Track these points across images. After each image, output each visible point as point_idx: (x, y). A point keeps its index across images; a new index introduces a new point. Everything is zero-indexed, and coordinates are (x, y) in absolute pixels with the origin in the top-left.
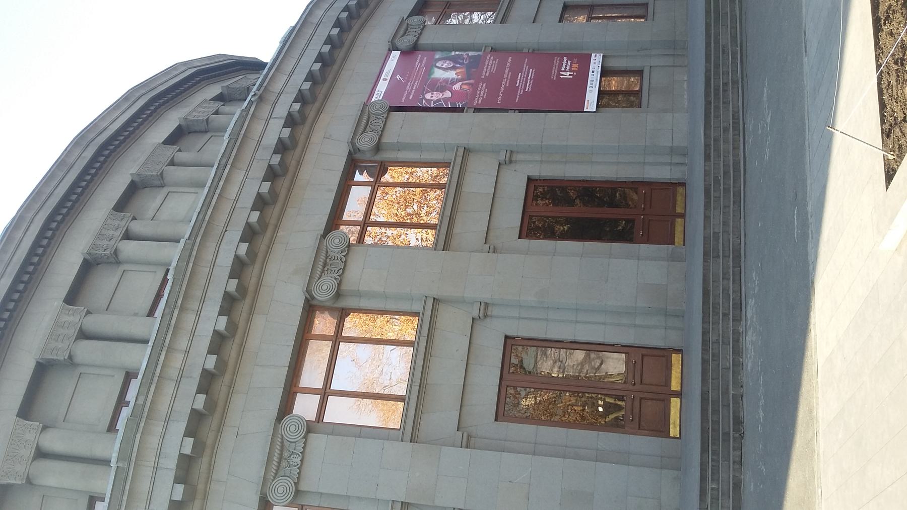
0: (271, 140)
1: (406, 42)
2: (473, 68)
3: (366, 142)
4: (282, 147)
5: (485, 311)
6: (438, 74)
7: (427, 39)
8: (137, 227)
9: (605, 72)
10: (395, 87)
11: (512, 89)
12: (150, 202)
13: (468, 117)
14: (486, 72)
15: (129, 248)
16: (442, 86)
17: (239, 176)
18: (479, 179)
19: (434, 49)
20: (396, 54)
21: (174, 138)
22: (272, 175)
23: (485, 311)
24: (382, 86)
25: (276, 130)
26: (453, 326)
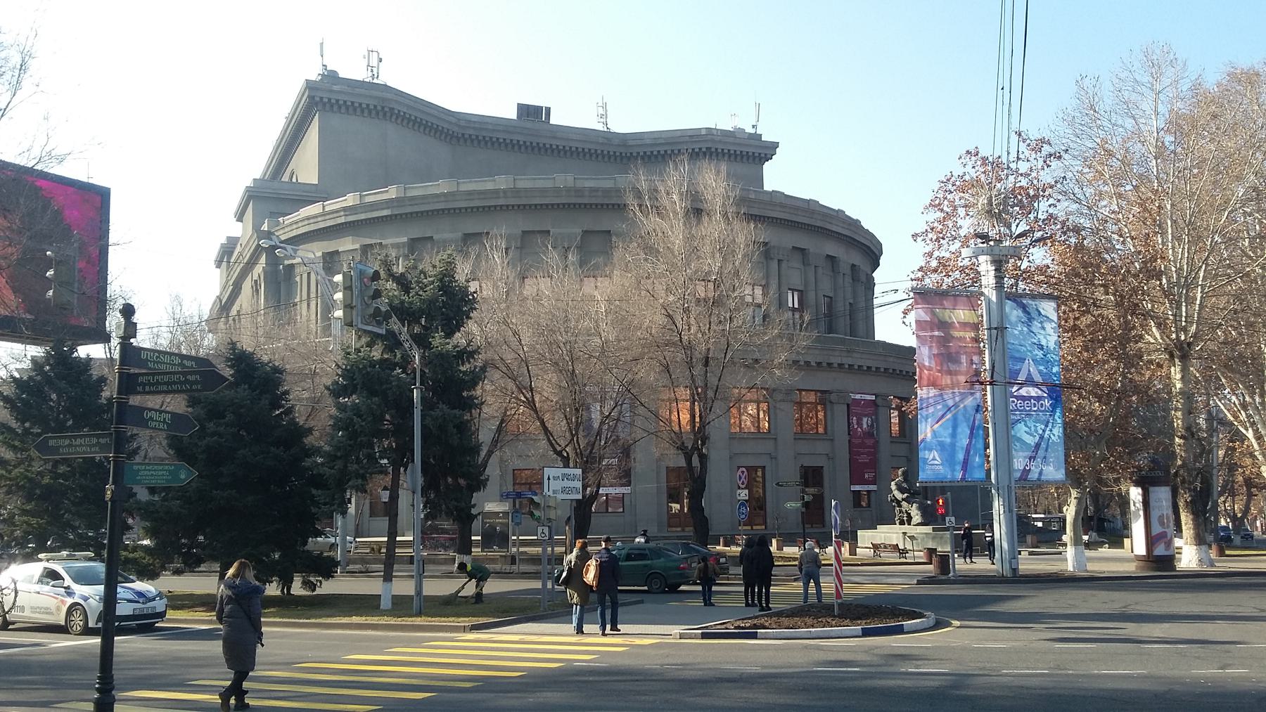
0: (832, 360)
1: (879, 402)
2: (869, 434)
3: (833, 397)
4: (829, 365)
5: (773, 458)
6: (865, 420)
7: (882, 411)
8: (784, 265)
9: (869, 492)
10: (857, 402)
11: (859, 454)
12: (796, 263)
13: (847, 438)
14: (866, 441)
15: (774, 265)
16: (860, 424)
17: (817, 352)
18: (822, 447)
19: (876, 414)
20: (873, 398)
21: (831, 258)
22: (819, 364)
23: (773, 458)
24: (858, 397)
25: (836, 360)
26: (768, 446)
